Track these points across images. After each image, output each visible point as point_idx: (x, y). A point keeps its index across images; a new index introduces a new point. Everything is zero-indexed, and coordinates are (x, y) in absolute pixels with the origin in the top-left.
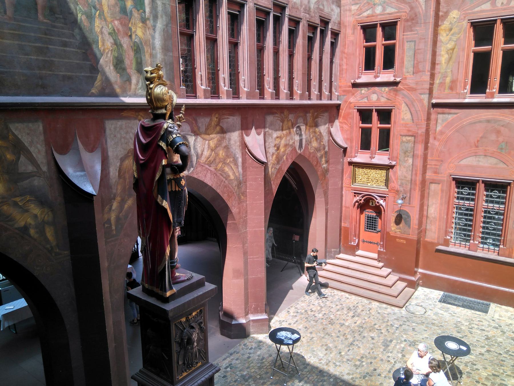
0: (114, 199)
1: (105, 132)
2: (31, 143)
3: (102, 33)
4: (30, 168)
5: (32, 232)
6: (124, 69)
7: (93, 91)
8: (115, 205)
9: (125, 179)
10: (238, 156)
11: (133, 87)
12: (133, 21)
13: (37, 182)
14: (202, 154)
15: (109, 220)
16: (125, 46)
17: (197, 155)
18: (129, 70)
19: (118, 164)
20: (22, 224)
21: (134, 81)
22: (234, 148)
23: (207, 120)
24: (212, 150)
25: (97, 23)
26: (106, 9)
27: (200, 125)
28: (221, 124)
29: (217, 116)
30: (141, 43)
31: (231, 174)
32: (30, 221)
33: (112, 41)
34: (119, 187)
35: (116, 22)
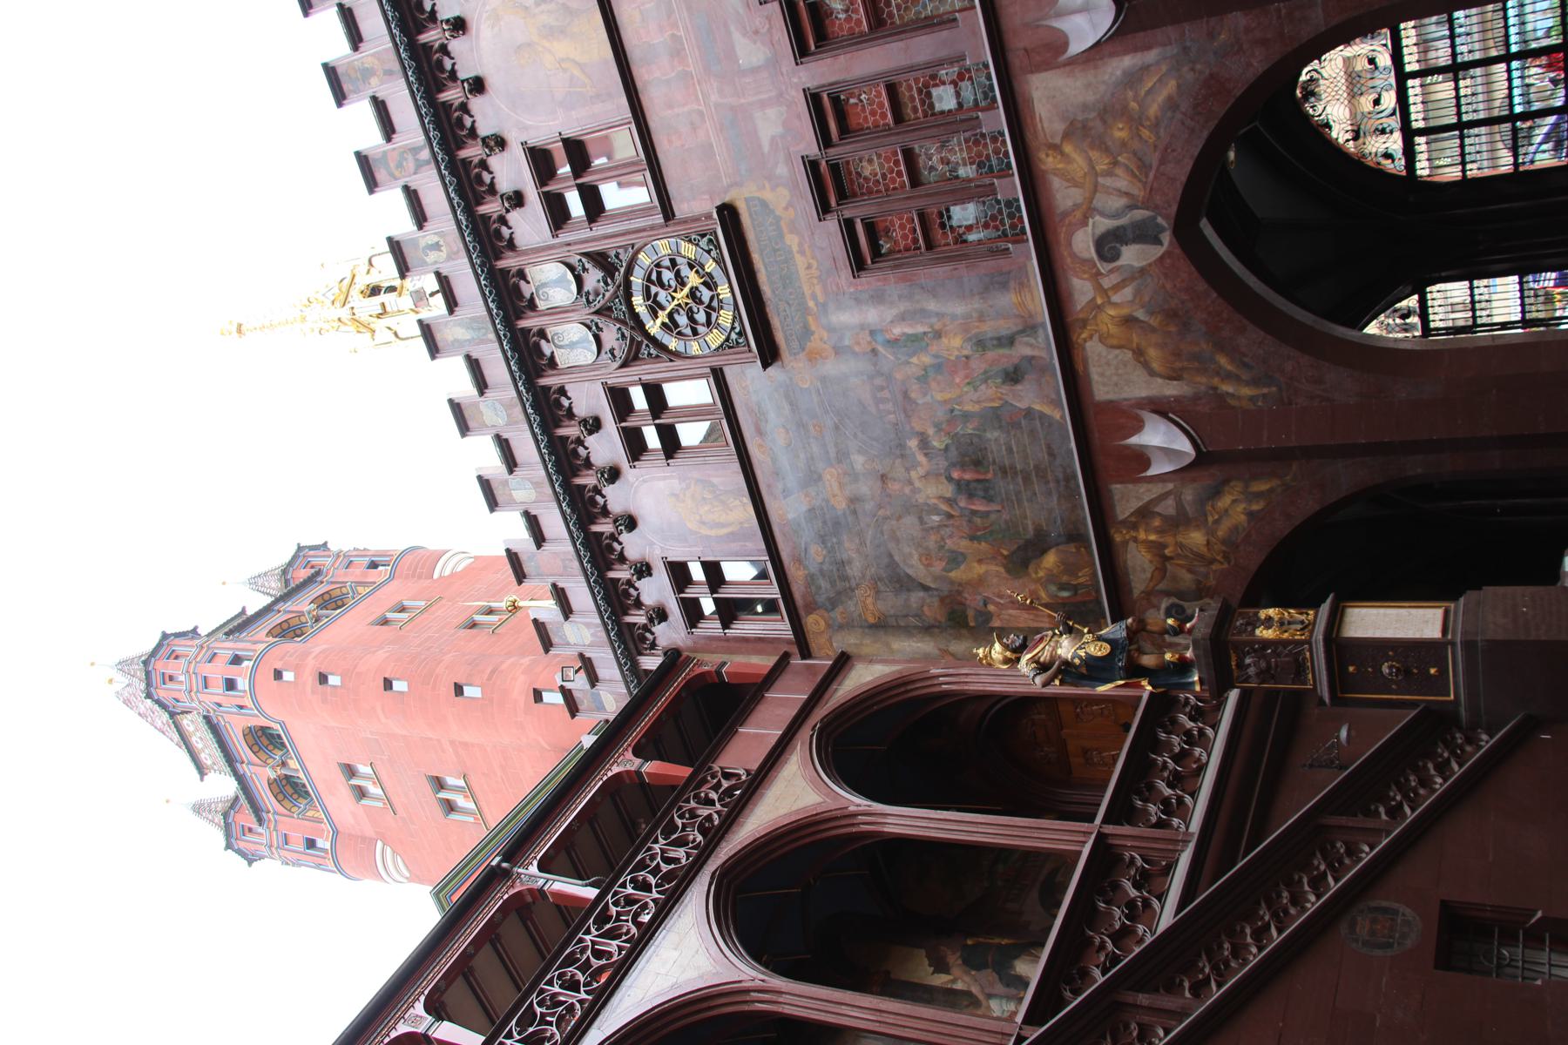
0: (1215, 389)
1: (1111, 402)
2: (1138, 498)
3: (978, 402)
4: (1170, 502)
5: (1255, 507)
6: (1016, 369)
7: (1057, 415)
8: (1228, 388)
9: (1182, 369)
10: (1119, 73)
11: (1036, 353)
12: (945, 354)
13: (1189, 495)
14: (1127, 194)
15: (1252, 399)
16: (984, 366)
17: (1131, 207)
18: (1016, 361)
19: (1160, 380)
20: (1243, 517)
21: (1028, 352)
22: (1102, 88)
23: (1056, 183)
24: (1115, 163)
25: (969, 407)
26: (948, 396)
27: (1069, 203)
28: (1057, 140)
29: (1043, 156)
30: (970, 339)
31: (1161, 98)
32: (1240, 507)
33: (983, 387)
34: (1198, 379)
35: (957, 380)
